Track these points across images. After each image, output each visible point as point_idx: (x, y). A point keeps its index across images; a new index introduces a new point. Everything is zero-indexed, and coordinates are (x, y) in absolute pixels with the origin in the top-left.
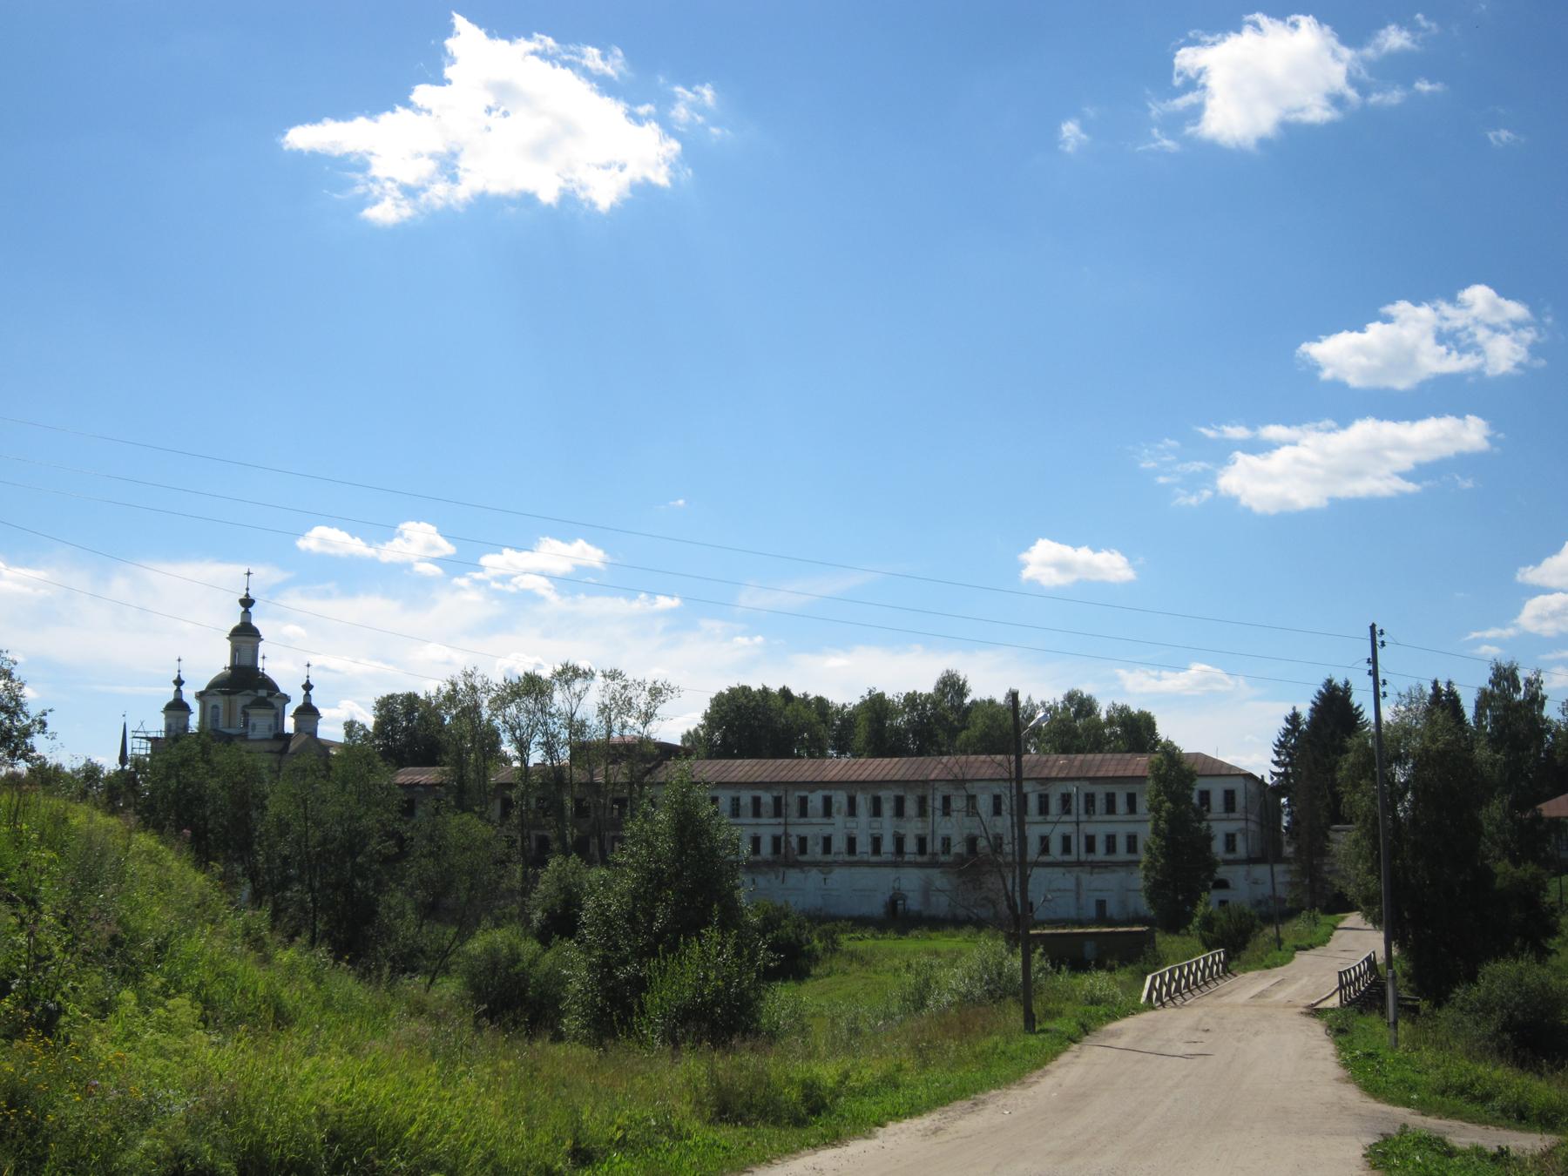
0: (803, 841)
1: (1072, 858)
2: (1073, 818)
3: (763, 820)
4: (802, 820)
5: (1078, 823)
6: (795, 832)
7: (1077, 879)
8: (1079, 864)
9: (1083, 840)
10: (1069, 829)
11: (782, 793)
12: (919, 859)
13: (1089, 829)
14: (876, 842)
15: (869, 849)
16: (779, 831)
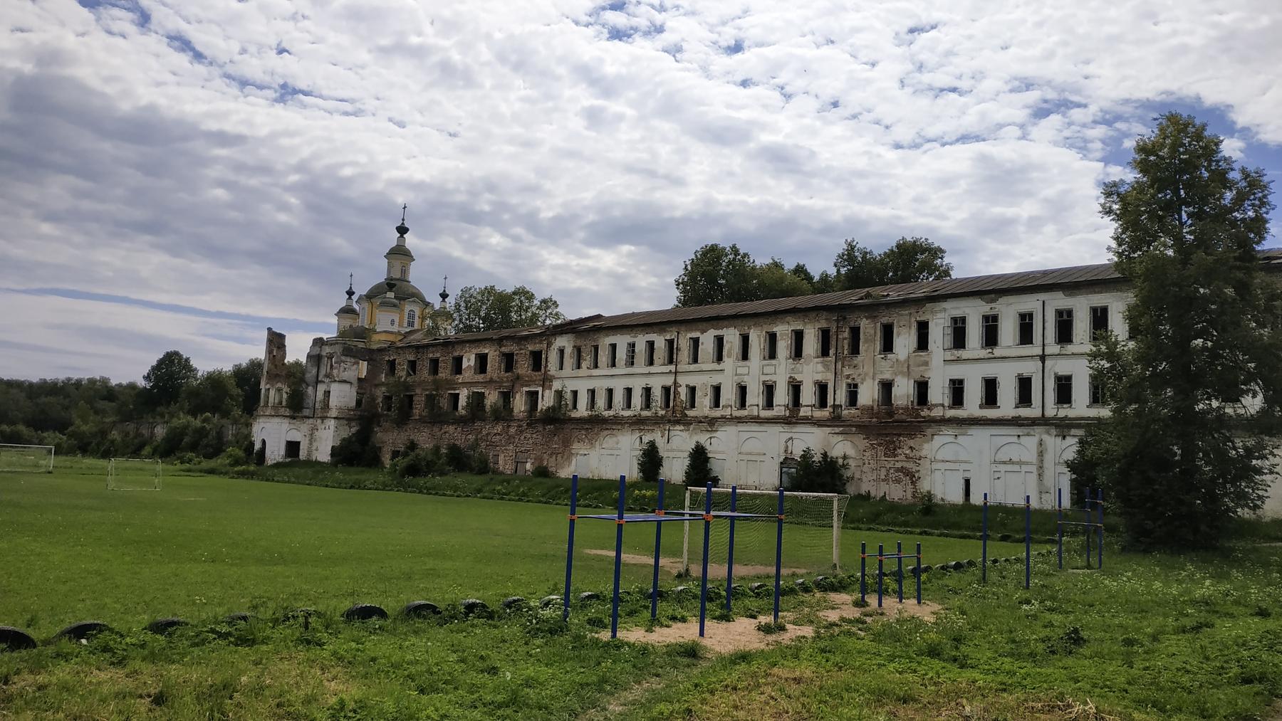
0: (692, 390)
1: (1033, 412)
2: (1037, 350)
3: (652, 369)
4: (693, 367)
5: (1043, 358)
6: (684, 381)
7: (1041, 443)
8: (1043, 421)
9: (1051, 385)
10: (1030, 368)
11: (673, 336)
12: (819, 414)
13: (1063, 367)
14: (769, 390)
15: (761, 401)
16: (669, 381)
